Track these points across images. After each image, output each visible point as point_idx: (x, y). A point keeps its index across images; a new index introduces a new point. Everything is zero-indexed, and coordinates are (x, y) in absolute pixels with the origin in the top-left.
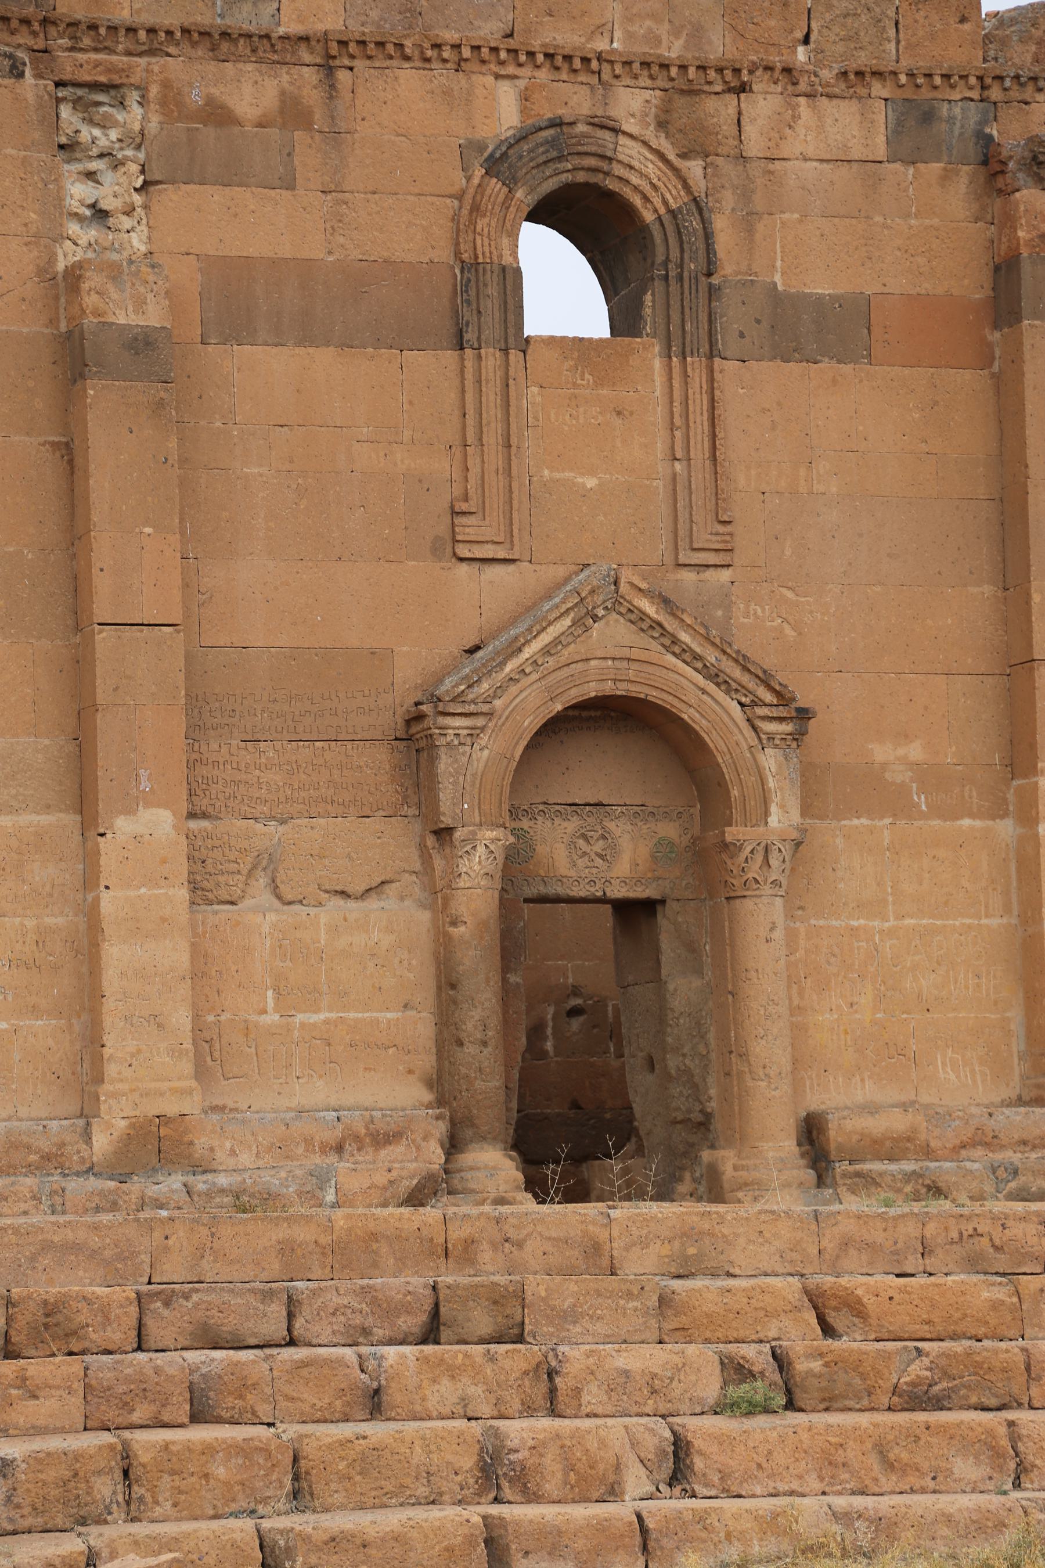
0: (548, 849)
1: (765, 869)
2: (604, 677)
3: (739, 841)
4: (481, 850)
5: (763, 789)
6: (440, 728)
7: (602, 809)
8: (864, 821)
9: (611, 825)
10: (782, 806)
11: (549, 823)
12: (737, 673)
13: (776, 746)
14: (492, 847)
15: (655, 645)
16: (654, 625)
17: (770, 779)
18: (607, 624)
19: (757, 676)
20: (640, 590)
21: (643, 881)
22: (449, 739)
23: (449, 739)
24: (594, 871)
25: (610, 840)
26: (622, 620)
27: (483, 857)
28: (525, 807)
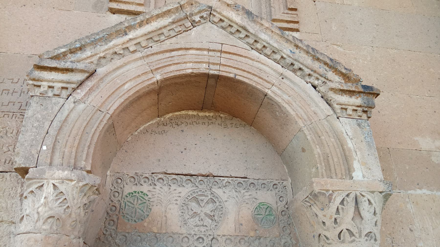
0: (163, 209)
1: (358, 221)
2: (199, 60)
3: (328, 191)
4: (48, 190)
5: (343, 150)
6: (34, 80)
7: (212, 180)
8: (424, 191)
9: (219, 192)
10: (364, 164)
11: (166, 188)
12: (309, 61)
13: (349, 117)
14: (62, 188)
15: (241, 44)
16: (240, 29)
17: (349, 141)
18: (204, 28)
19: (326, 64)
20: (228, 5)
21: (246, 239)
22: (42, 89)
23: (42, 89)
24: (203, 229)
25: (218, 204)
26: (215, 27)
27: (51, 198)
28: (147, 175)
